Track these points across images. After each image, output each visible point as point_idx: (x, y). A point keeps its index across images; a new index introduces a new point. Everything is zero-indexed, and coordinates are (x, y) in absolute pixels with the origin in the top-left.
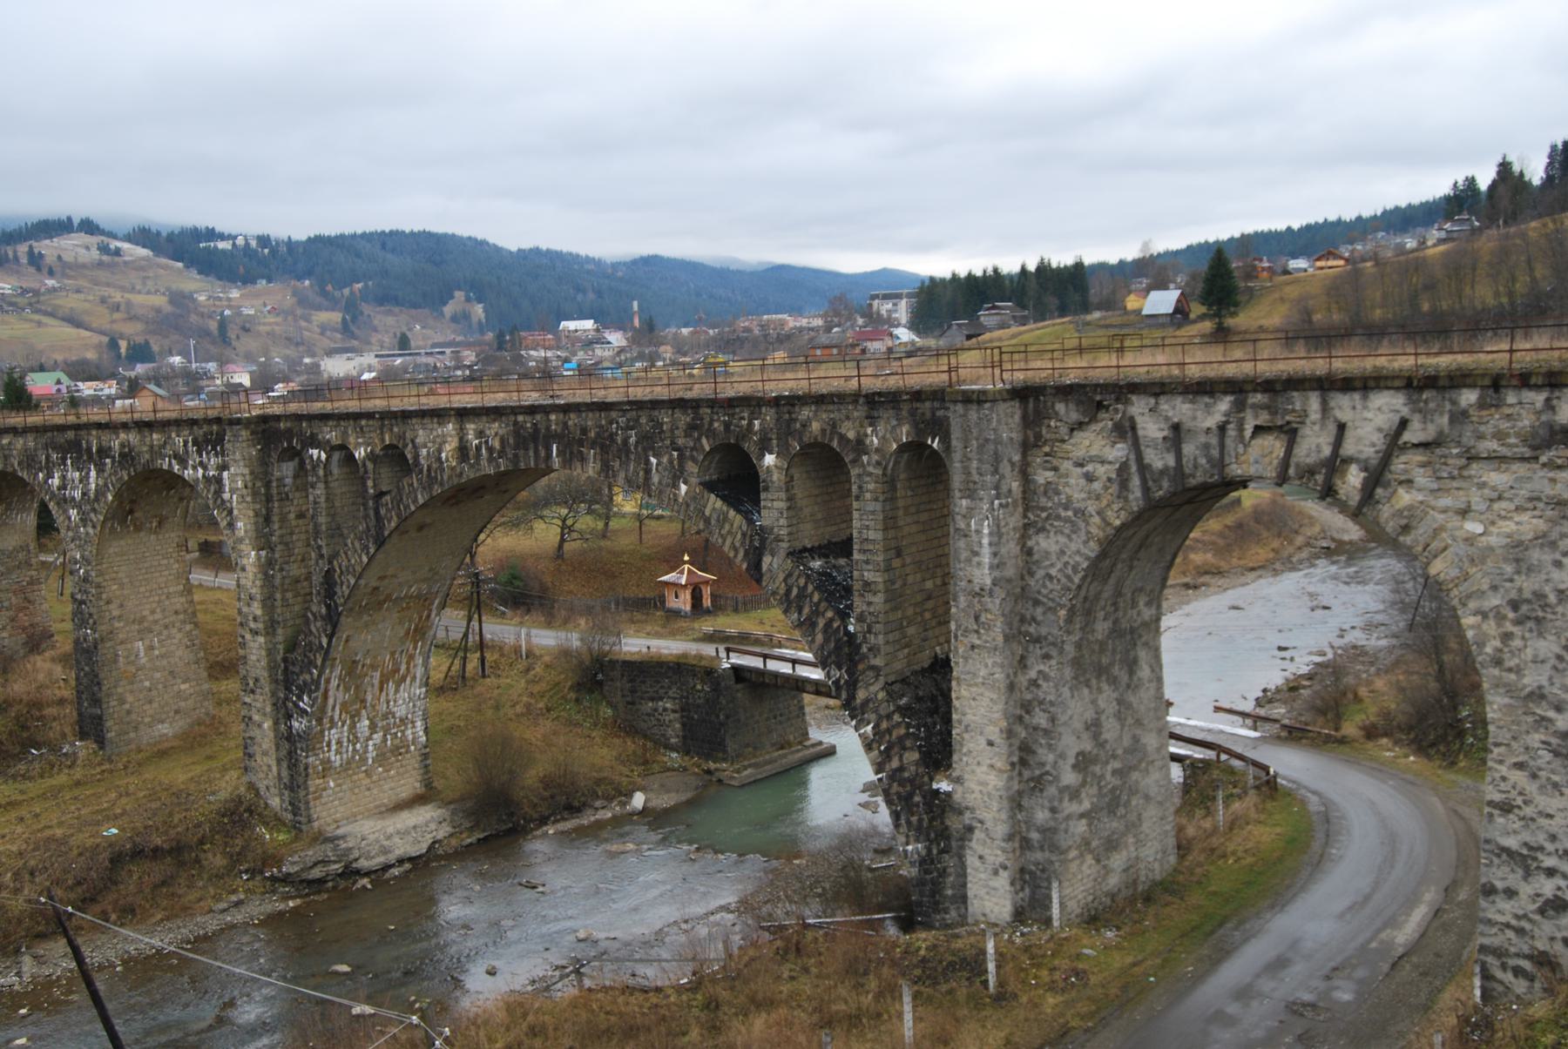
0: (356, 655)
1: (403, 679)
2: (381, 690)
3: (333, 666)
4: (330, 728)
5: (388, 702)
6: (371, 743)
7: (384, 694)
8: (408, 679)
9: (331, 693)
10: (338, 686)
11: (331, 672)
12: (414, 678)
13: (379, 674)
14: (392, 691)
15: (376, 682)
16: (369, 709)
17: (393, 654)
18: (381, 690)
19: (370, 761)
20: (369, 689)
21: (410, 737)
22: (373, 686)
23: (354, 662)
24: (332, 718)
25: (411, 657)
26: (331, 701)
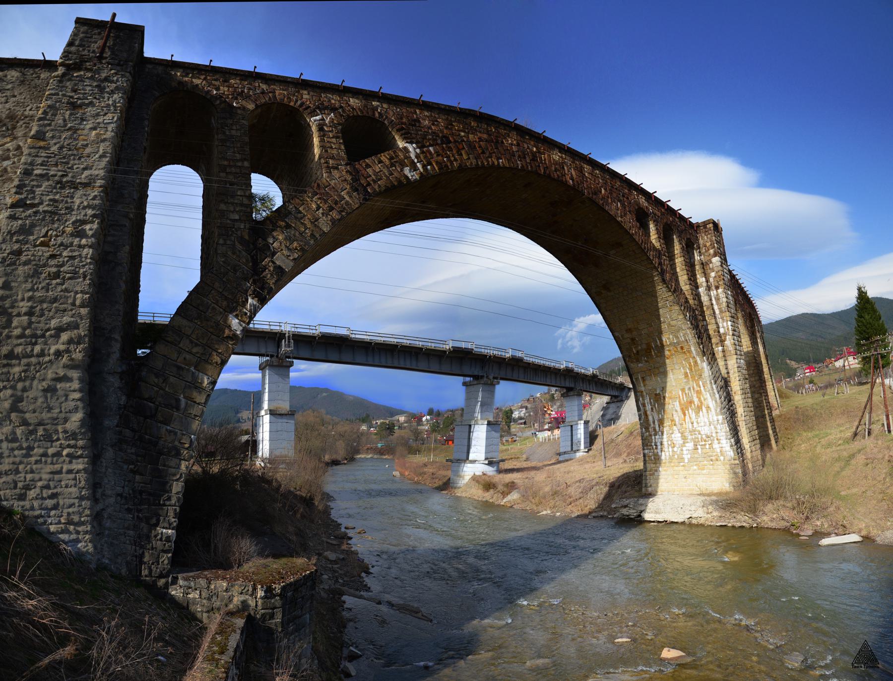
0: (656, 390)
1: (699, 409)
2: (685, 414)
3: (643, 396)
4: (655, 435)
5: (692, 423)
6: (684, 449)
7: (687, 417)
8: (703, 408)
9: (649, 413)
10: (652, 409)
11: (643, 400)
12: (708, 407)
13: (678, 403)
14: (693, 416)
15: (678, 409)
16: (679, 426)
17: (683, 390)
18: (685, 414)
19: (686, 461)
20: (674, 413)
21: (718, 450)
22: (676, 411)
23: (656, 395)
24: (655, 429)
25: (699, 393)
26: (650, 418)
